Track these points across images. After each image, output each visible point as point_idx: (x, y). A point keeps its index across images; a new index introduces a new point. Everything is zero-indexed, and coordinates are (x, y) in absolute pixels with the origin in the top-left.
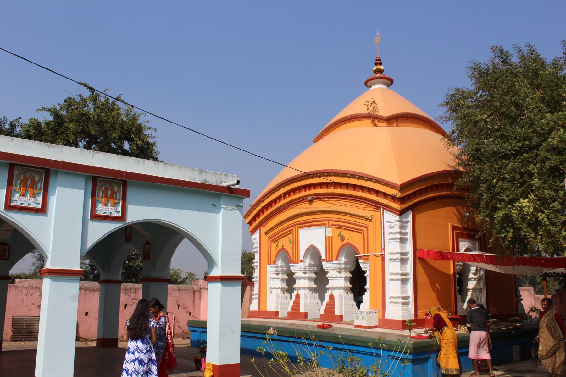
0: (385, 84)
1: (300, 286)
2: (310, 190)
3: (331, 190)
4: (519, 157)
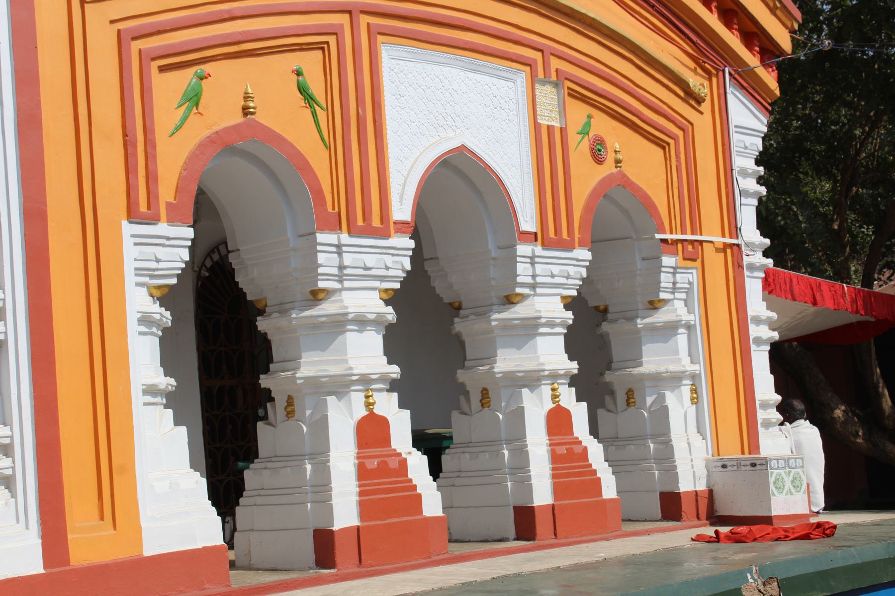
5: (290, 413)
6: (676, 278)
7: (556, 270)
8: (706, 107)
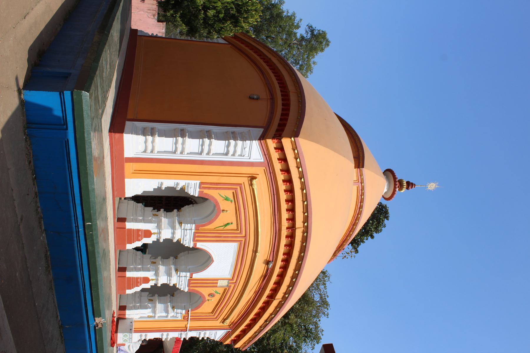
5: (154, 215)
6: (180, 313)
7: (183, 282)
8: (221, 324)
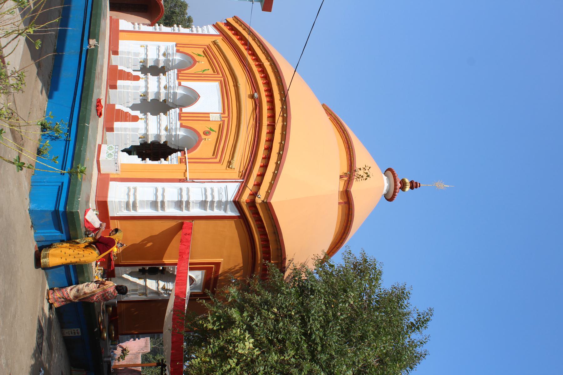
0: (388, 192)
1: (149, 81)
2: (266, 96)
3: (265, 122)
4: (304, 338)
7: (174, 118)
